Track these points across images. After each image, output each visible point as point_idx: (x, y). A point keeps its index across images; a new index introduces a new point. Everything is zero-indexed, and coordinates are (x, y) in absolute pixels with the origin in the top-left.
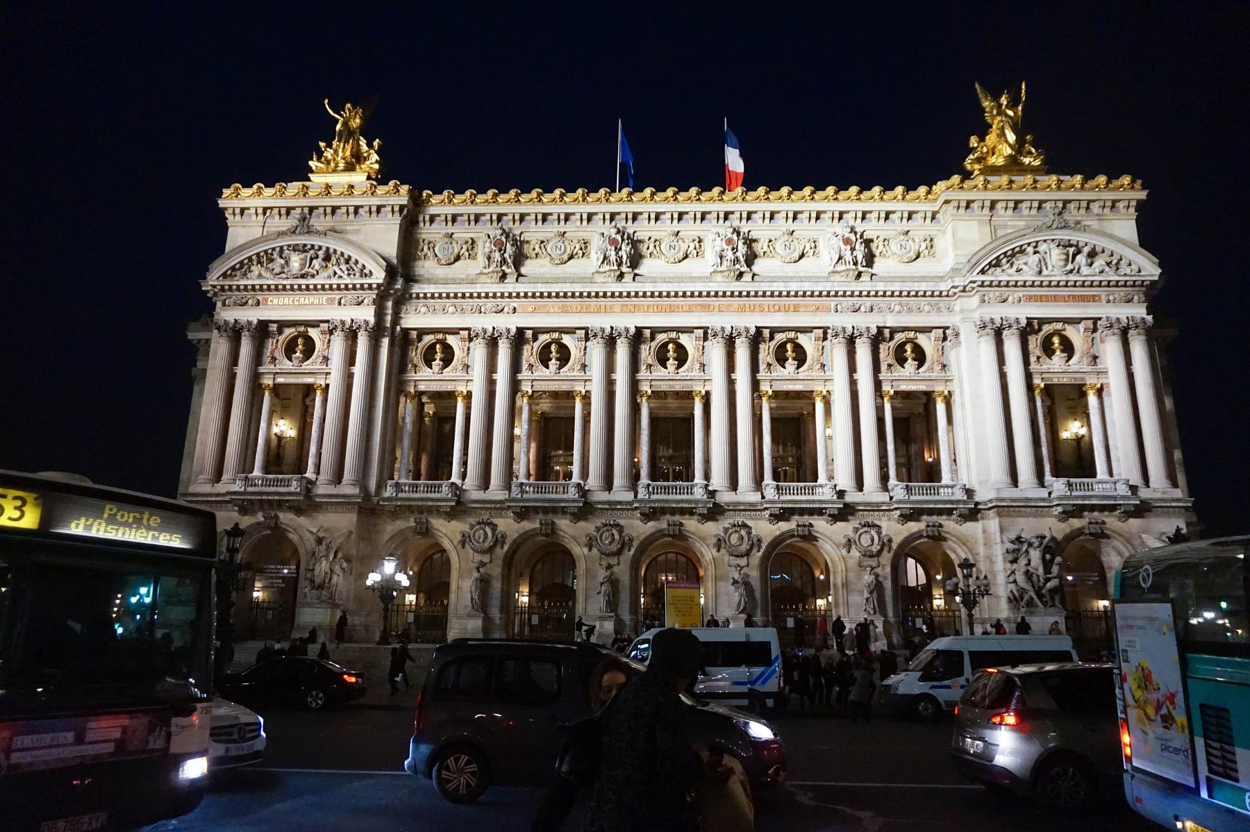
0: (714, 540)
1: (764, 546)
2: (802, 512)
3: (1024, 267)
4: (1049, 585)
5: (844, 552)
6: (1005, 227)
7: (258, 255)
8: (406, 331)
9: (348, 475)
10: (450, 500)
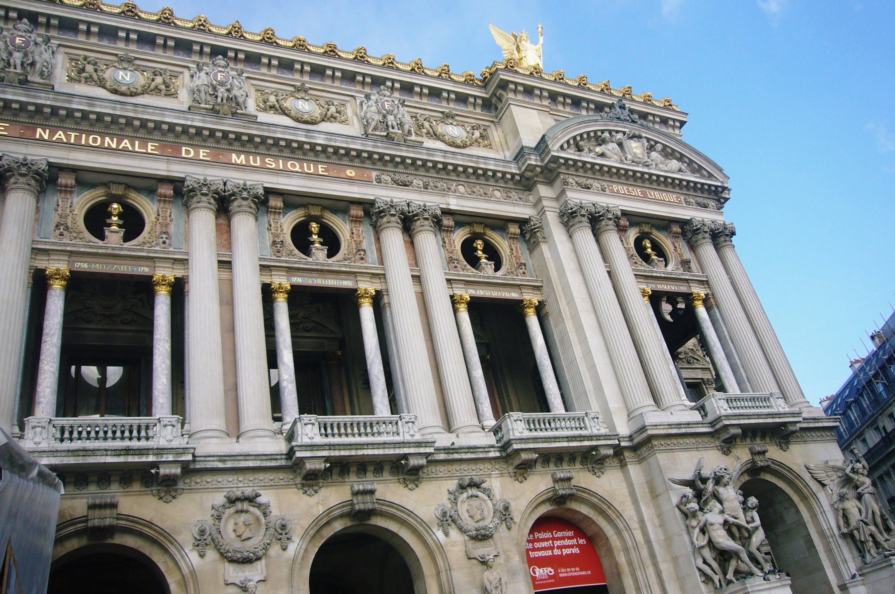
0: (195, 531)
1: (296, 539)
3: (607, 152)
5: (440, 535)
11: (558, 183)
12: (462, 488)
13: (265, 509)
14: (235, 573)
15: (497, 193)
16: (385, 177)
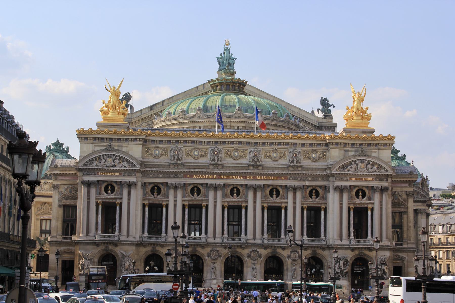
2: (275, 247)
3: (350, 169)
4: (345, 271)
5: (287, 259)
6: (348, 151)
7: (95, 157)
8: (145, 183)
9: (131, 234)
10: (164, 242)
11: (334, 178)
12: (293, 251)
13: (258, 252)
14: (253, 262)
15: (320, 179)
16: (291, 179)
